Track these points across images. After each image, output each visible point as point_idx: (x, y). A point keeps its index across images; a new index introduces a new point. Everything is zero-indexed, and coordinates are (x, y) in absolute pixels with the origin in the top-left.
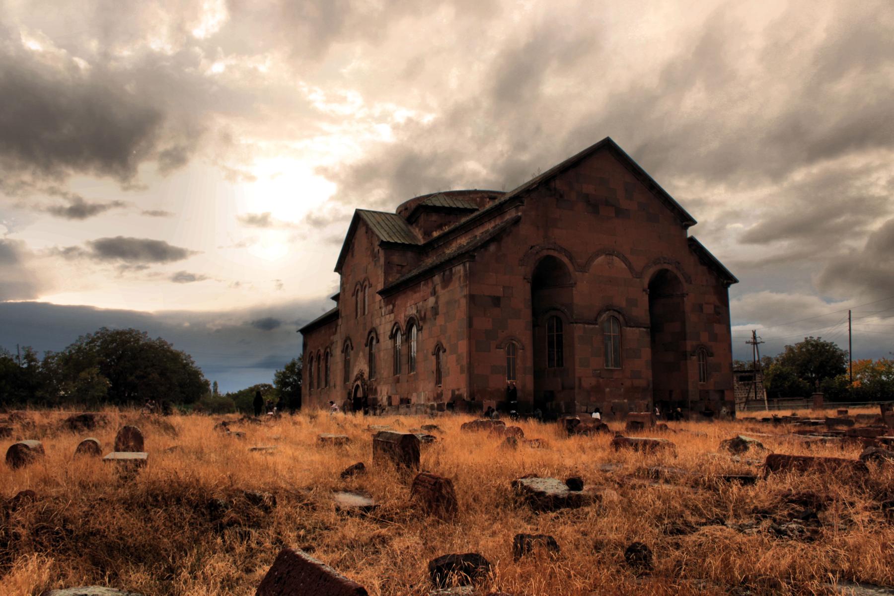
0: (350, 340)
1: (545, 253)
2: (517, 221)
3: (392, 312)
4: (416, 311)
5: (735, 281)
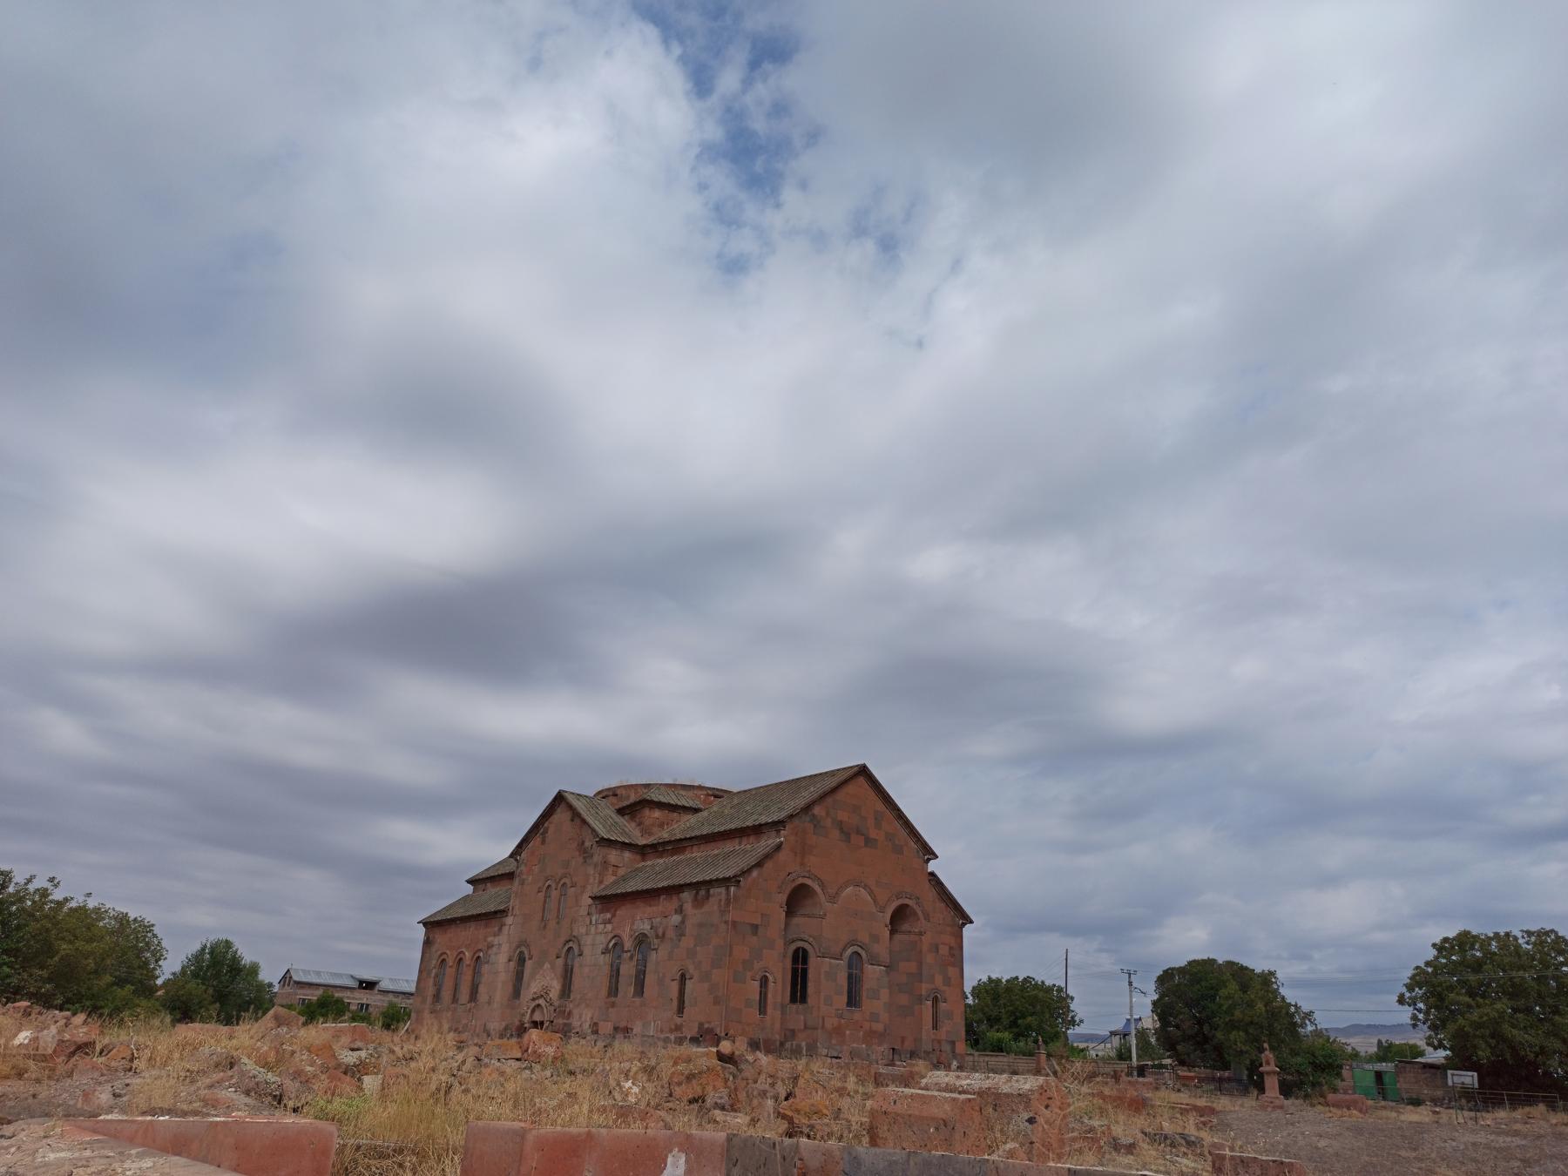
0: (528, 946)
1: (801, 881)
2: (779, 847)
3: (609, 922)
4: (649, 927)
5: (971, 922)
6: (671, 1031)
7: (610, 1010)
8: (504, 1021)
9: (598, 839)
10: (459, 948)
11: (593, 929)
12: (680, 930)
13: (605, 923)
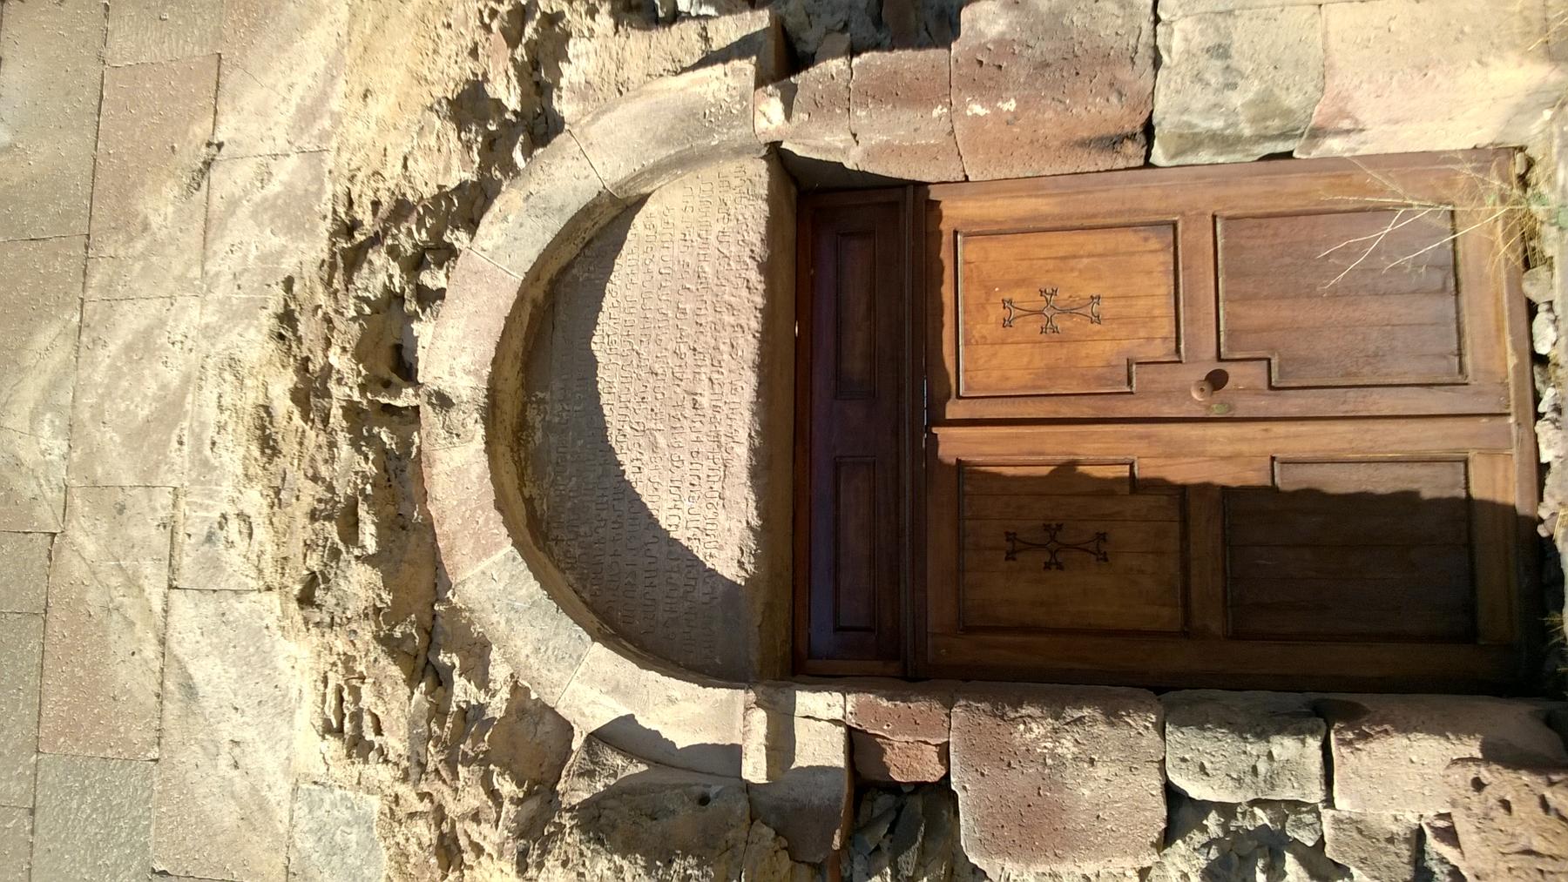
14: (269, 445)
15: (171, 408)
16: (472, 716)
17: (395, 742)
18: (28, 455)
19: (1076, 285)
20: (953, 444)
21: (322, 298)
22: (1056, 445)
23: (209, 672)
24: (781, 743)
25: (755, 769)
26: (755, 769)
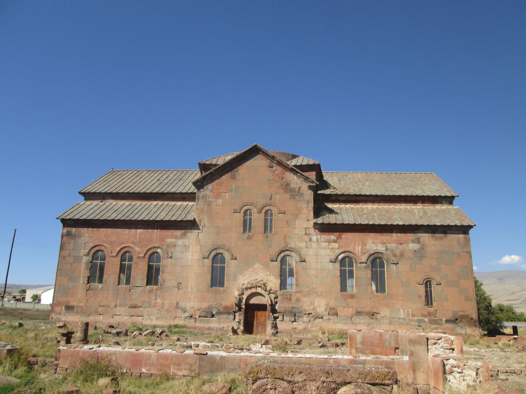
3: (335, 241)
4: (384, 249)
6: (424, 316)
7: (349, 300)
8: (205, 302)
9: (311, 184)
10: (122, 243)
11: (314, 245)
12: (420, 254)
13: (329, 242)
14: (256, 280)
15: (258, 274)
16: (244, 291)
17: (242, 287)
18: (256, 265)
19: (263, 317)
20: (256, 312)
21: (263, 282)
22: (256, 316)
23: (245, 277)
24: (243, 305)
25: (242, 304)
26: (242, 304)
